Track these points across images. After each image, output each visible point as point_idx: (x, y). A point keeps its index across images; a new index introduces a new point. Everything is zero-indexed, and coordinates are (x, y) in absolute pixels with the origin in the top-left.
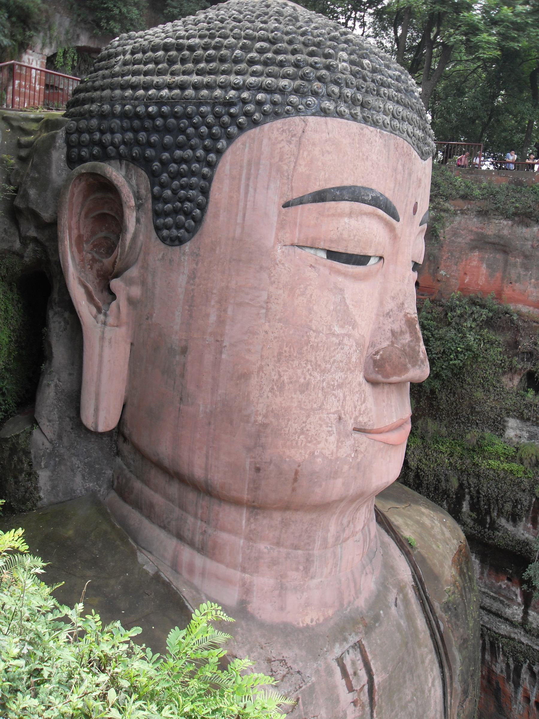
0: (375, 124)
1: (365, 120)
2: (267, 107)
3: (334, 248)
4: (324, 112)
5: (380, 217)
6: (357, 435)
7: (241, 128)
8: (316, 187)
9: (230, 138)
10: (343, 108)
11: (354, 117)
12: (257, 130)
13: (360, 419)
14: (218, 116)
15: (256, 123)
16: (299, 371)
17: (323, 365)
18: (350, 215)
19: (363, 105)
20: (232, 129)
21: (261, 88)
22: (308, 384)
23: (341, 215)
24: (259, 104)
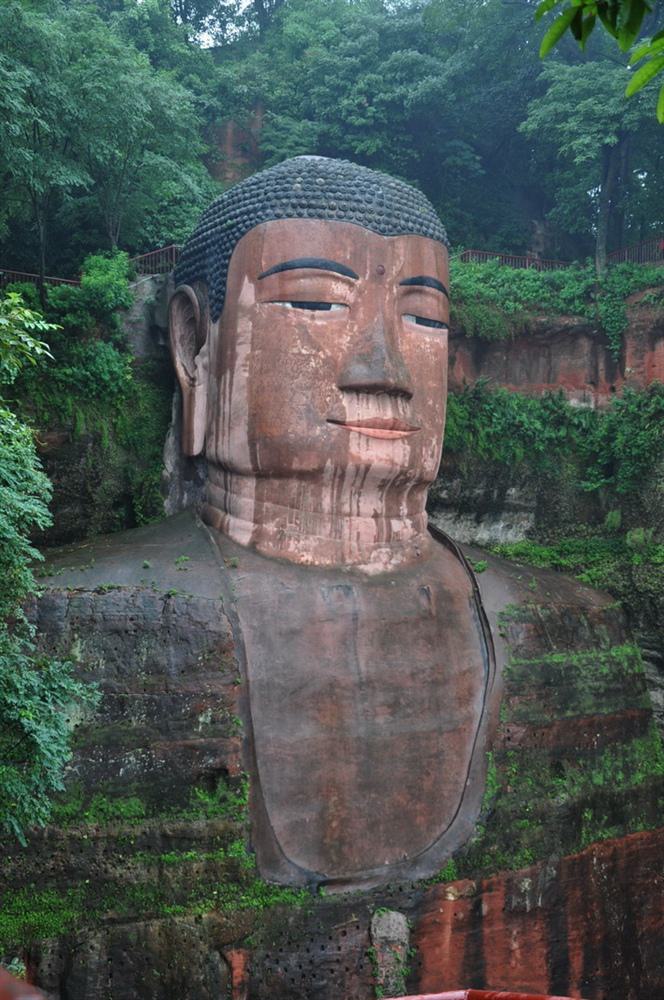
0: (320, 216)
1: (311, 216)
2: (248, 223)
3: (294, 300)
4: (278, 216)
5: (337, 279)
6: (330, 424)
7: (237, 239)
8: (278, 261)
9: (233, 246)
10: (290, 210)
11: (300, 215)
12: (243, 238)
13: (333, 413)
14: (228, 236)
15: (243, 234)
16: (274, 379)
17: (292, 374)
18: (304, 276)
19: (310, 206)
20: (234, 241)
21: (242, 214)
22: (280, 386)
23: (298, 277)
24: (244, 221)
